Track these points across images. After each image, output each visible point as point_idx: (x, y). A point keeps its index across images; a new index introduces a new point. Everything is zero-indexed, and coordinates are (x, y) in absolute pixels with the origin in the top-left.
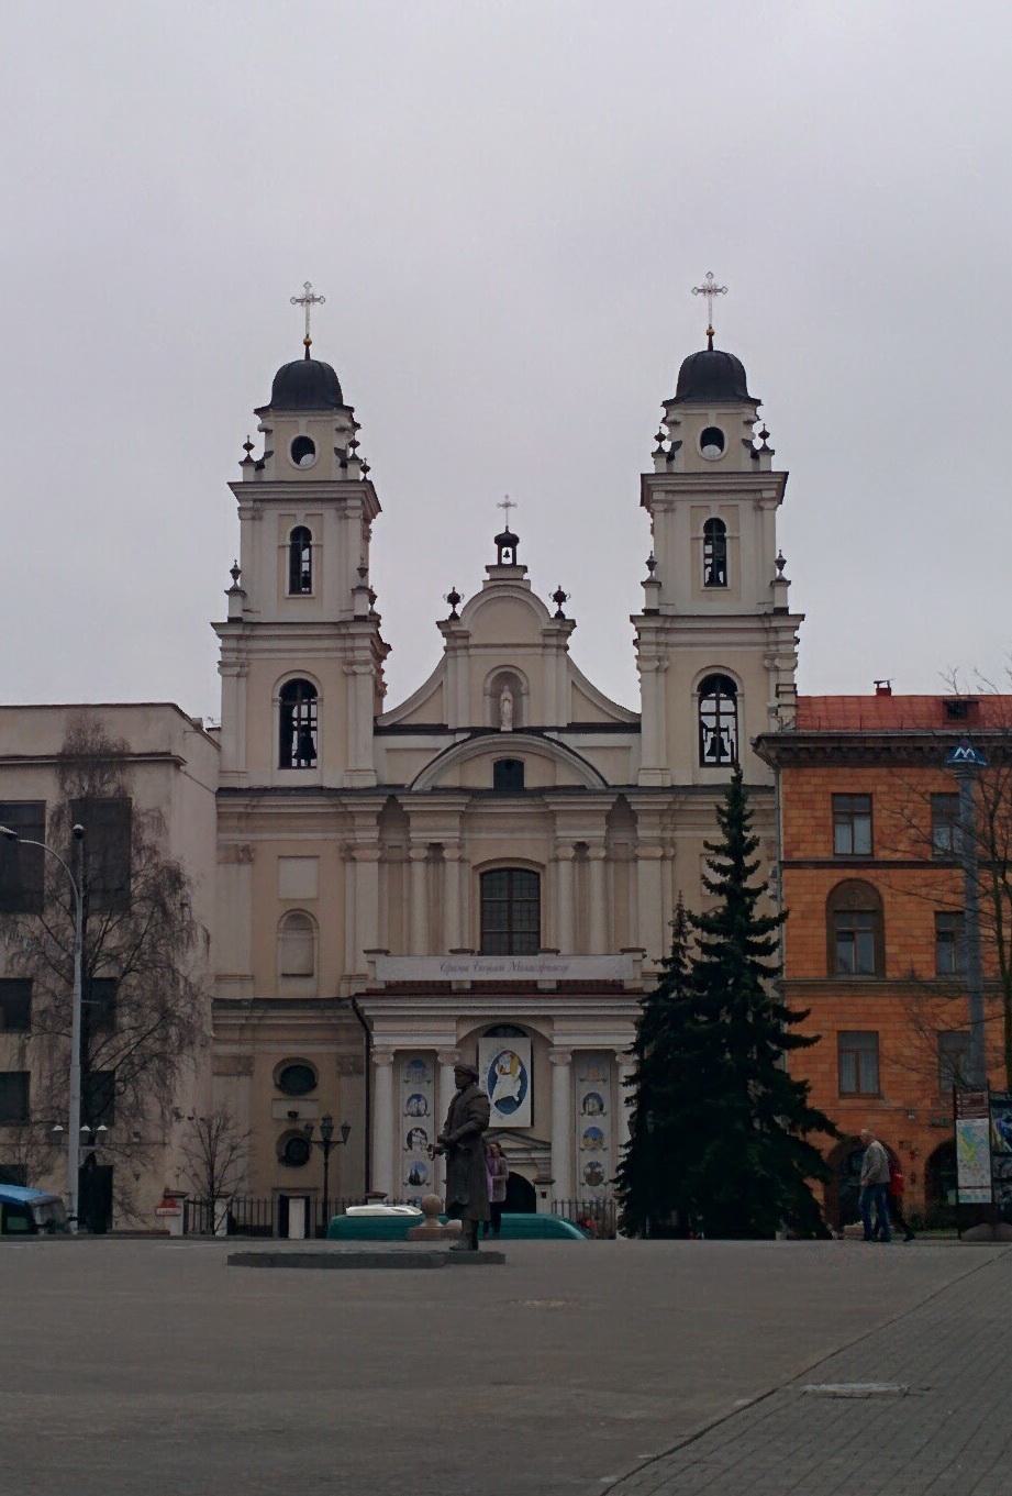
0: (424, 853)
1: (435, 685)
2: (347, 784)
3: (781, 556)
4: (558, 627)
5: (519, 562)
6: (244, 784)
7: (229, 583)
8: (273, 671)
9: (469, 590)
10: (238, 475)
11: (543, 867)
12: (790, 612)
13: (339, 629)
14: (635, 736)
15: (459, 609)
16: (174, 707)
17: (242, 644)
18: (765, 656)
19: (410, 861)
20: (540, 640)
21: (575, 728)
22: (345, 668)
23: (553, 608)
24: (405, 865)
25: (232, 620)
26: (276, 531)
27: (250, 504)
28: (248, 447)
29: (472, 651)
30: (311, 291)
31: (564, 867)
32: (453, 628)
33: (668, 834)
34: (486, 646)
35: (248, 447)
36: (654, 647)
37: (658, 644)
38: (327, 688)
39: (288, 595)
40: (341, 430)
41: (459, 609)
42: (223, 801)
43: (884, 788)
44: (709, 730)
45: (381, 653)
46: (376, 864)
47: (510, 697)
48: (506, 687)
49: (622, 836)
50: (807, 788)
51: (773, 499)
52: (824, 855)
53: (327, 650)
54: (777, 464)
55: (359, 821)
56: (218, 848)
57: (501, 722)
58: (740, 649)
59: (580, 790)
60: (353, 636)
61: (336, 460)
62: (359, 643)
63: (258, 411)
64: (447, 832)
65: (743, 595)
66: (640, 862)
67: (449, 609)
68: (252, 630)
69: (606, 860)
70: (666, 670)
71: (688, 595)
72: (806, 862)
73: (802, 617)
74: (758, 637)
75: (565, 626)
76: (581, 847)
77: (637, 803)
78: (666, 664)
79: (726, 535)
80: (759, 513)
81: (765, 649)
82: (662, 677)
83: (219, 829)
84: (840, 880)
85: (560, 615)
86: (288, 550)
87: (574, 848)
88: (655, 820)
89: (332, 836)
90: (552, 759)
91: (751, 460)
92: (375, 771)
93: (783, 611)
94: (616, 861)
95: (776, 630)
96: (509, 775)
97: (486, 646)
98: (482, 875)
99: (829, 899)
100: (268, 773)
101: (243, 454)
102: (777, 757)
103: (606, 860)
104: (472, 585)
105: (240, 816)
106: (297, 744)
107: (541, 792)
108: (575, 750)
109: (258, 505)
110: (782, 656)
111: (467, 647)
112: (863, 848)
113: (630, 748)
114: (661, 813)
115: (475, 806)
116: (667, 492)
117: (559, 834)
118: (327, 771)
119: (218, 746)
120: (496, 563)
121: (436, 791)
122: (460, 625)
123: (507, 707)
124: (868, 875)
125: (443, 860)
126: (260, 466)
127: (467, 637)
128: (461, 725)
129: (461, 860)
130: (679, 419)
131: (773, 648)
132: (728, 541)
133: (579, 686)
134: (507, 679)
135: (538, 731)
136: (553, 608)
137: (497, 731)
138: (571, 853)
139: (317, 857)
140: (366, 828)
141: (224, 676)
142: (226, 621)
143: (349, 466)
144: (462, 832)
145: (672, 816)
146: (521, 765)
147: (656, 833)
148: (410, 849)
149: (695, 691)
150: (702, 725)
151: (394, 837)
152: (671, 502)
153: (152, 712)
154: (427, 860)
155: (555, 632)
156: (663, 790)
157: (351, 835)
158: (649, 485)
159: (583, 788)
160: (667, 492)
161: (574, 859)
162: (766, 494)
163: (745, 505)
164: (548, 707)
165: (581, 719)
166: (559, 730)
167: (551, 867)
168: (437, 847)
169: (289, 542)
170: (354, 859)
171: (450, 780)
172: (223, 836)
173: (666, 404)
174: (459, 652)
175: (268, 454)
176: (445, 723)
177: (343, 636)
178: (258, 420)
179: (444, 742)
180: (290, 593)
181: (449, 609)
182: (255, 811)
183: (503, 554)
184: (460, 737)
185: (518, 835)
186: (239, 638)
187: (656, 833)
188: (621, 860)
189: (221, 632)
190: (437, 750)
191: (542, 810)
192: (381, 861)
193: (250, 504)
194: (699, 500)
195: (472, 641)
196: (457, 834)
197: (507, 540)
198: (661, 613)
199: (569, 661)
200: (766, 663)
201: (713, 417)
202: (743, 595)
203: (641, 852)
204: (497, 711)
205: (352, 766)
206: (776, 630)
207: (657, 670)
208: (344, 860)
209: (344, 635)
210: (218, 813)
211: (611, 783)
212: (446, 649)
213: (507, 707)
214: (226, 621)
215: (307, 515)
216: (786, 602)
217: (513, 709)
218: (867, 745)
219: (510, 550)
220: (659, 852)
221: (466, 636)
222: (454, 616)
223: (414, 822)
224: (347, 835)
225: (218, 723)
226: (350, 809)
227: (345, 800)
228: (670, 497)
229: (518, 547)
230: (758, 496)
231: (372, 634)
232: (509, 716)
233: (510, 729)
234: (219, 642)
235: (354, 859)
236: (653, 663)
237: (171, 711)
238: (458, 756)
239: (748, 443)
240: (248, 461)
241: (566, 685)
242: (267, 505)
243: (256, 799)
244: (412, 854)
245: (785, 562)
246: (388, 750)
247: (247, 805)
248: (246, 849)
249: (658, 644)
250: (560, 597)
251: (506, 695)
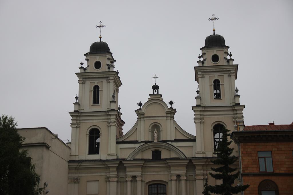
0: (130, 179)
1: (134, 129)
2: (108, 158)
3: (237, 89)
4: (171, 111)
5: (159, 93)
6: (77, 159)
7: (75, 101)
8: (87, 125)
9: (143, 102)
10: (79, 71)
11: (167, 183)
12: (240, 104)
13: (106, 113)
14: (194, 143)
15: (141, 108)
16: (47, 129)
17: (78, 118)
18: (233, 118)
19: (126, 181)
20: (165, 115)
21: (176, 141)
22: (108, 124)
23: (169, 106)
24: (125, 183)
25: (75, 111)
26: (89, 87)
27: (82, 79)
28: (82, 64)
29: (145, 119)
30: (102, 24)
31: (173, 182)
32: (140, 112)
33: (205, 172)
34: (149, 117)
35: (82, 64)
36: (199, 116)
37: (200, 115)
38: (103, 132)
39: (92, 105)
40: (109, 59)
41: (142, 106)
42: (71, 164)
43: (276, 149)
44: (217, 142)
45: (122, 123)
46: (116, 182)
47: (157, 132)
48: (156, 129)
49: (191, 173)
50: (249, 150)
51: (233, 73)
52: (256, 171)
53: (103, 119)
54: (234, 63)
55: (111, 169)
56: (68, 179)
57: (154, 139)
58: (225, 116)
59: (178, 159)
60: (110, 115)
61: (107, 67)
62: (112, 117)
63: (85, 55)
64: (137, 172)
65: (226, 100)
66: (196, 180)
67: (139, 107)
68: (81, 114)
69: (186, 180)
70: (203, 123)
71: (209, 101)
72: (250, 174)
73: (244, 106)
75: (173, 111)
76: (178, 176)
77: (195, 163)
78: (203, 121)
79: (220, 84)
80: (230, 77)
81: (233, 116)
82: (202, 124)
83: (69, 173)
84: (263, 180)
85: (171, 108)
86: (92, 92)
87: (177, 177)
88: (201, 168)
89: (103, 174)
90: (169, 150)
91: (227, 63)
92: (116, 154)
93: (238, 104)
94: (189, 181)
95: (236, 110)
96: (156, 155)
97: (149, 117)
98: (149, 186)
99: (259, 186)
100: (85, 155)
101: (80, 66)
102: (238, 139)
103: (186, 180)
104: (145, 99)
105: (75, 169)
106: (94, 148)
107: (166, 160)
108: (177, 147)
109: (84, 79)
110: (238, 118)
111: (144, 118)
112: (270, 170)
113: (193, 146)
114: (203, 165)
115: (146, 164)
116: (202, 72)
117: (171, 172)
118: (102, 155)
119: (70, 148)
120: (152, 94)
121: (134, 160)
122: (142, 111)
123: (156, 135)
124: (273, 178)
125: (137, 181)
126: (85, 69)
127: (144, 115)
128: (142, 141)
129: (142, 181)
130: (205, 52)
131: (235, 115)
132: (221, 86)
133: (177, 128)
134: (156, 127)
135: (165, 142)
136: (169, 106)
137: (153, 142)
138: (175, 178)
139: (99, 181)
140: (112, 172)
141: (72, 127)
142: (73, 111)
143: (110, 68)
144: (142, 172)
145: (206, 166)
146: (161, 152)
147: (202, 172)
148: (126, 177)
149: (212, 129)
150: (215, 141)
151: (122, 174)
152: (203, 75)
153: (38, 130)
154: (131, 181)
155: (170, 113)
156: (203, 158)
157: (108, 174)
158: (197, 70)
159: (179, 158)
160: (202, 72)
161: (176, 180)
162: (231, 72)
163: (226, 76)
164: (168, 134)
165: (177, 138)
166: (172, 141)
167: (169, 183)
168: (134, 177)
169: (92, 89)
170: (109, 181)
171: (139, 157)
172: (70, 175)
173: (201, 49)
174: (142, 119)
175: (88, 66)
176: (137, 140)
177: (107, 115)
178: (85, 57)
179: (137, 146)
180: (93, 104)
181: (139, 107)
182: (80, 167)
183: (155, 91)
184: (142, 144)
185: (159, 173)
186: (77, 116)
187: (202, 172)
188: (191, 180)
189: (72, 115)
190: (135, 148)
191: (167, 165)
192: (117, 182)
193: (82, 79)
194: (211, 74)
195: (145, 116)
196: (141, 173)
197: (156, 87)
198: (201, 106)
199: (174, 121)
200: (234, 120)
201: (215, 52)
202: (226, 100)
203: (197, 177)
204: (153, 136)
205: (109, 153)
206: (236, 110)
207: (200, 123)
208: (106, 181)
209: (107, 115)
210: (69, 168)
211: (187, 157)
212: (138, 118)
213: (156, 135)
214: (73, 111)
215: (98, 82)
216: (239, 101)
217: (158, 135)
218: (269, 135)
219: (156, 90)
220: (202, 177)
221: (143, 114)
222: (140, 109)
223: (128, 169)
224: (107, 174)
225: (70, 141)
226: (108, 166)
227: (106, 163)
228: (203, 73)
230: (229, 72)
231: (116, 114)
232: (157, 137)
233: (157, 141)
234: (71, 118)
235: (109, 181)
236: (199, 120)
237: (44, 130)
238: (141, 149)
239: (226, 58)
240: (81, 68)
241: (173, 129)
242: (86, 80)
243: (80, 163)
244: (127, 179)
246: (120, 148)
247: (77, 165)
248: (77, 179)
249: (200, 115)
250: (171, 103)
251: (156, 131)
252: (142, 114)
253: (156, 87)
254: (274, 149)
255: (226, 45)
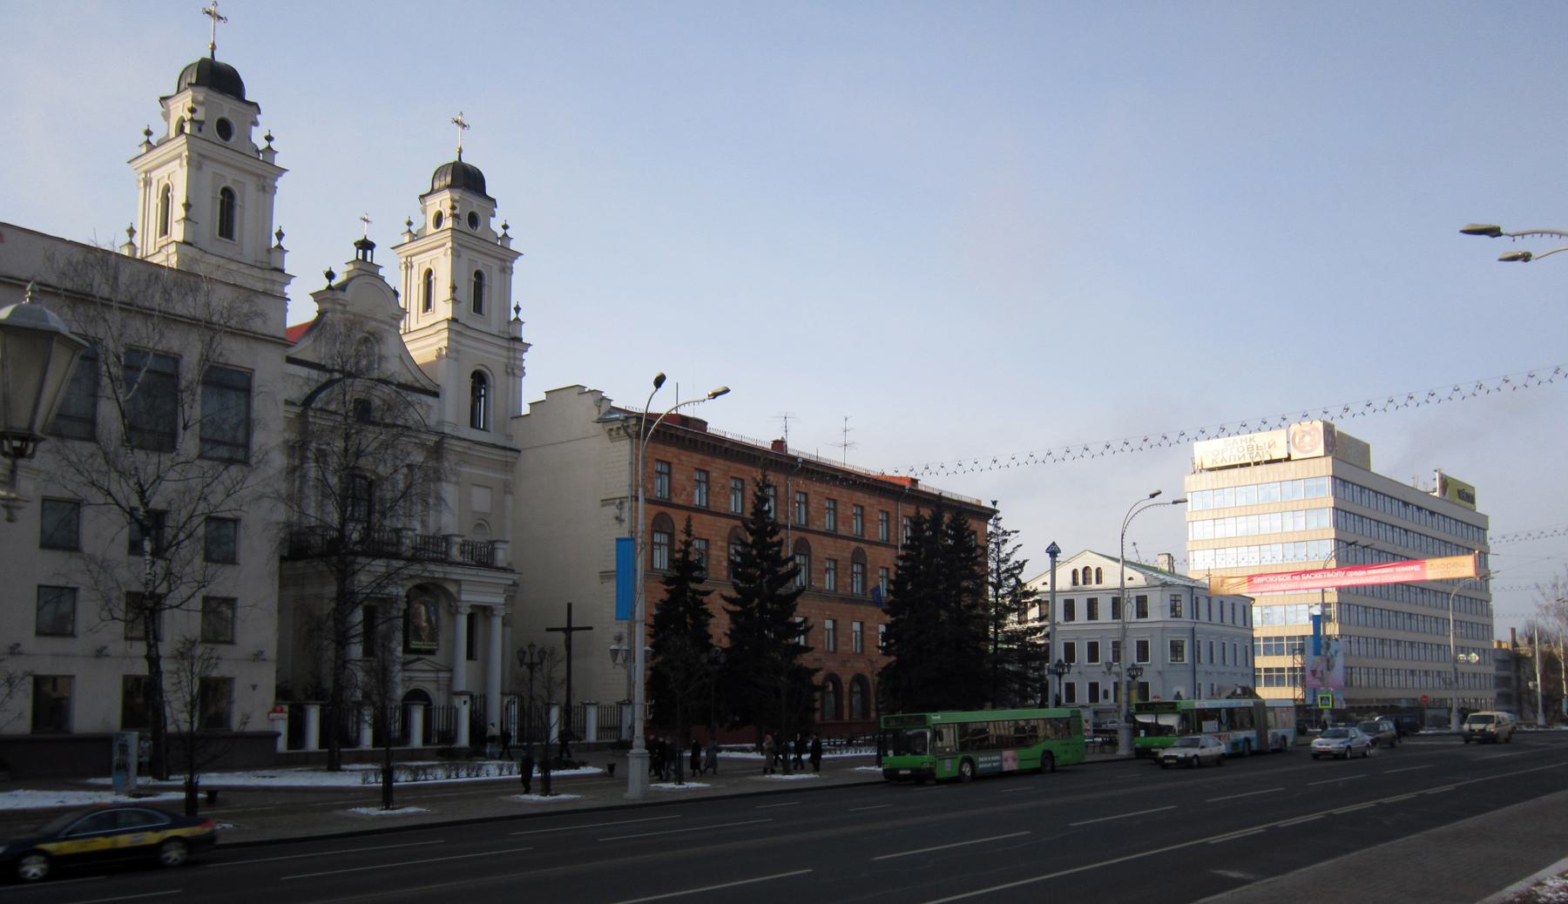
14: (436, 399)
73: (530, 345)
74: (505, 353)
86: (219, 202)
95: (515, 350)
124: (670, 511)
131: (512, 361)
181: (326, 283)
222: (330, 288)
229: (375, 250)
245: (520, 309)
252: (345, 303)
253: (366, 245)
254: (675, 461)
255: (489, 192)
